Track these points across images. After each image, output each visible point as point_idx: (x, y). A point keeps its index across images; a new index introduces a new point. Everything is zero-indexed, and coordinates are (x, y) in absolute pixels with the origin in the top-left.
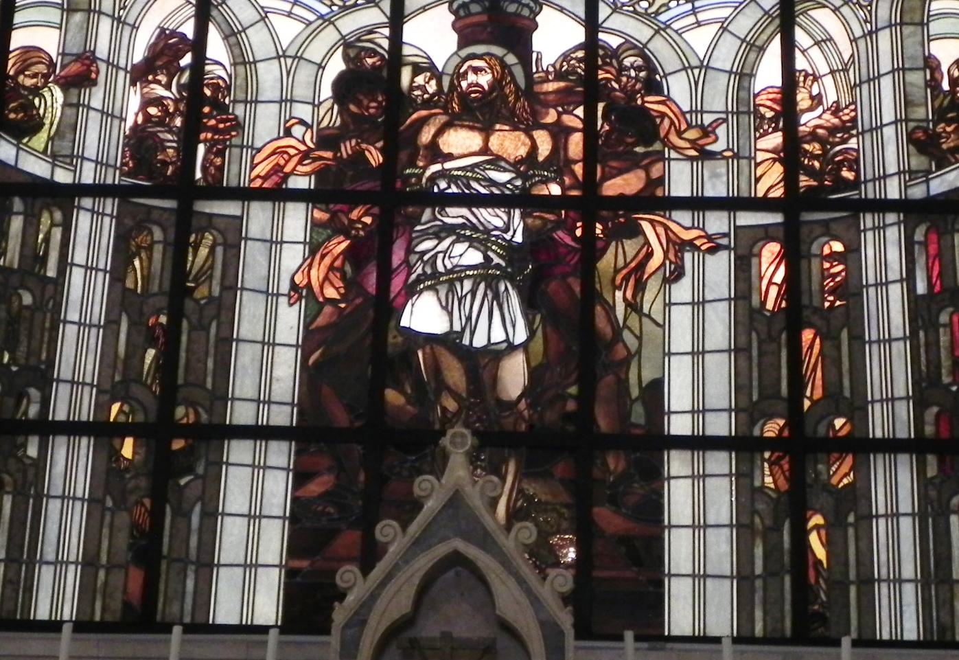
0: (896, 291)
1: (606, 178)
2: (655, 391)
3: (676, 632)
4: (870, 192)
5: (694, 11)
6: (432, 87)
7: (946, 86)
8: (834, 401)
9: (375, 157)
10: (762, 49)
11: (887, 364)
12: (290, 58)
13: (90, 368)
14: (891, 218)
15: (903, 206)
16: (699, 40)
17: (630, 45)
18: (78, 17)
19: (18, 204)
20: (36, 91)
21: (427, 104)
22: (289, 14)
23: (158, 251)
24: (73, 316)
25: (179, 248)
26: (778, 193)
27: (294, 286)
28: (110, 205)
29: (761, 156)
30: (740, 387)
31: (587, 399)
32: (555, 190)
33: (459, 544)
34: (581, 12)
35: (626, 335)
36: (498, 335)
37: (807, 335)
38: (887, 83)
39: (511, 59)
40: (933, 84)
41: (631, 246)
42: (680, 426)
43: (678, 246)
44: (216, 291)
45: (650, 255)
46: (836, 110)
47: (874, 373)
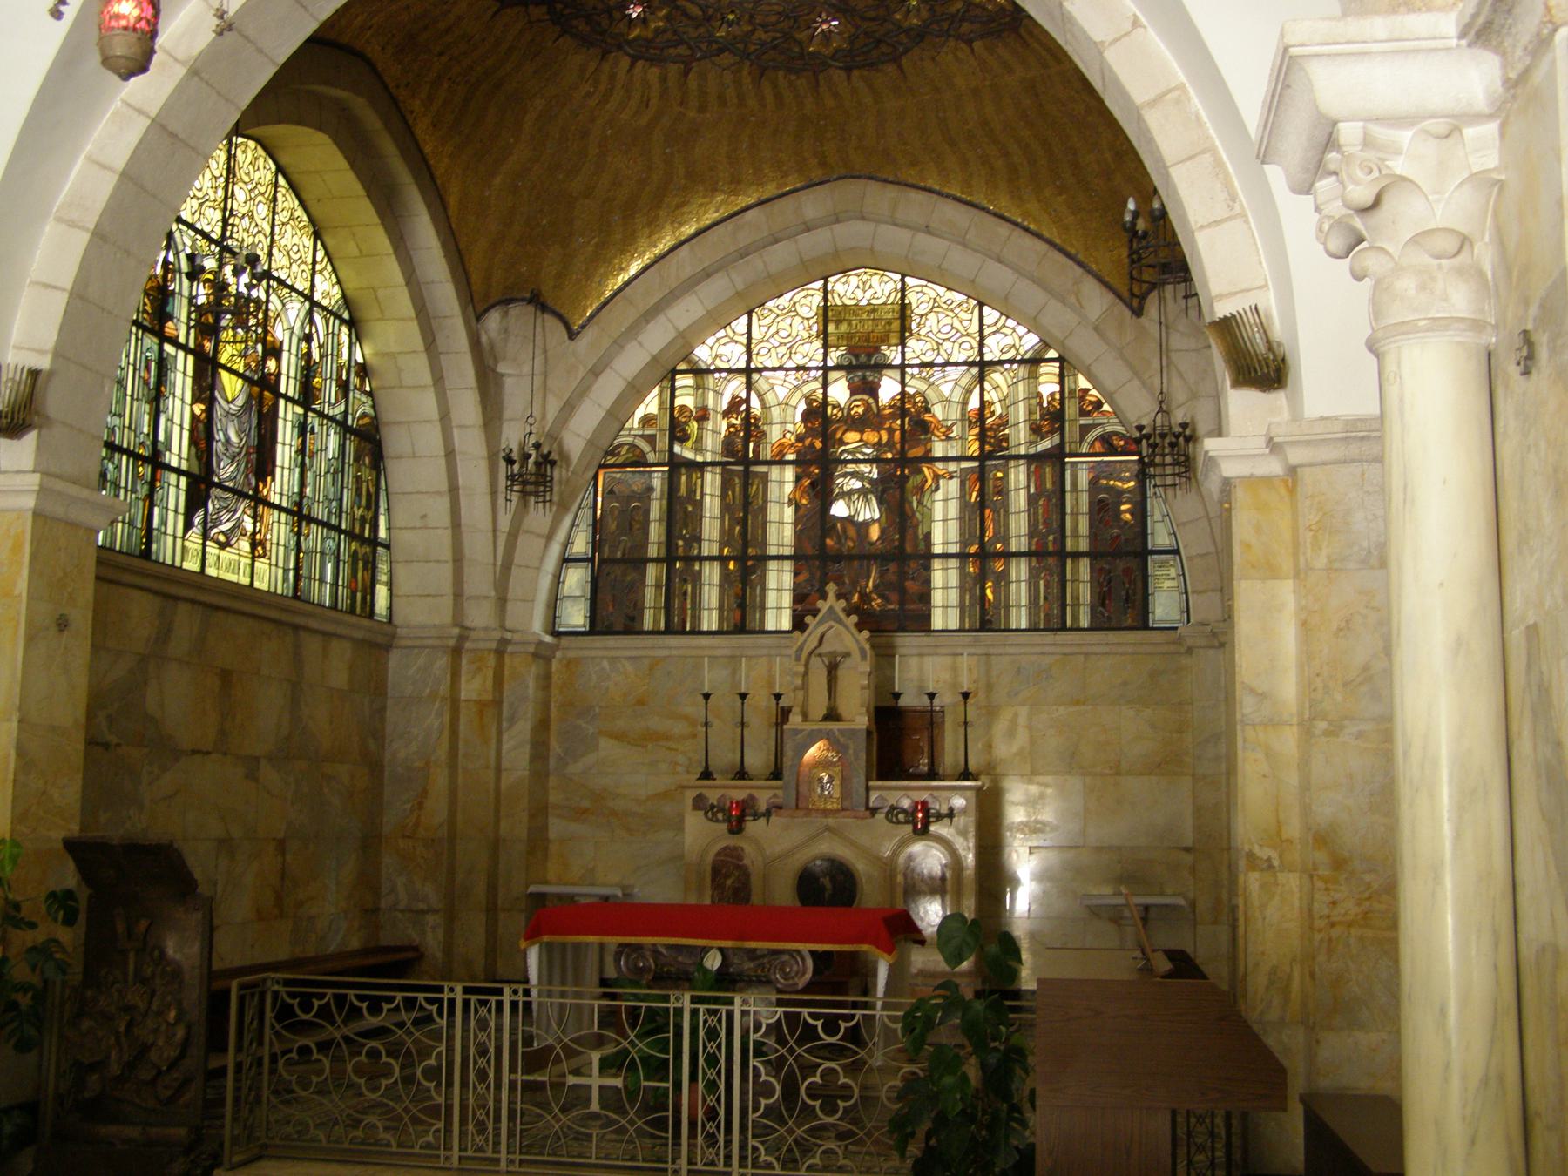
0: (1022, 492)
1: (910, 449)
2: (928, 536)
4: (1013, 452)
6: (840, 414)
7: (1045, 405)
8: (997, 537)
9: (818, 445)
10: (971, 392)
11: (1018, 522)
13: (715, 535)
14: (1021, 462)
15: (1027, 457)
16: (946, 389)
17: (918, 393)
19: (683, 470)
20: (686, 423)
21: (839, 421)
23: (737, 489)
25: (746, 486)
26: (976, 454)
27: (790, 500)
28: (718, 470)
31: (902, 540)
32: (889, 456)
33: (832, 623)
34: (899, 378)
35: (918, 515)
36: (868, 516)
37: (987, 511)
38: (1021, 404)
39: (871, 401)
40: (1040, 404)
41: (919, 478)
42: (937, 550)
43: (937, 477)
44: (760, 502)
46: (1000, 417)
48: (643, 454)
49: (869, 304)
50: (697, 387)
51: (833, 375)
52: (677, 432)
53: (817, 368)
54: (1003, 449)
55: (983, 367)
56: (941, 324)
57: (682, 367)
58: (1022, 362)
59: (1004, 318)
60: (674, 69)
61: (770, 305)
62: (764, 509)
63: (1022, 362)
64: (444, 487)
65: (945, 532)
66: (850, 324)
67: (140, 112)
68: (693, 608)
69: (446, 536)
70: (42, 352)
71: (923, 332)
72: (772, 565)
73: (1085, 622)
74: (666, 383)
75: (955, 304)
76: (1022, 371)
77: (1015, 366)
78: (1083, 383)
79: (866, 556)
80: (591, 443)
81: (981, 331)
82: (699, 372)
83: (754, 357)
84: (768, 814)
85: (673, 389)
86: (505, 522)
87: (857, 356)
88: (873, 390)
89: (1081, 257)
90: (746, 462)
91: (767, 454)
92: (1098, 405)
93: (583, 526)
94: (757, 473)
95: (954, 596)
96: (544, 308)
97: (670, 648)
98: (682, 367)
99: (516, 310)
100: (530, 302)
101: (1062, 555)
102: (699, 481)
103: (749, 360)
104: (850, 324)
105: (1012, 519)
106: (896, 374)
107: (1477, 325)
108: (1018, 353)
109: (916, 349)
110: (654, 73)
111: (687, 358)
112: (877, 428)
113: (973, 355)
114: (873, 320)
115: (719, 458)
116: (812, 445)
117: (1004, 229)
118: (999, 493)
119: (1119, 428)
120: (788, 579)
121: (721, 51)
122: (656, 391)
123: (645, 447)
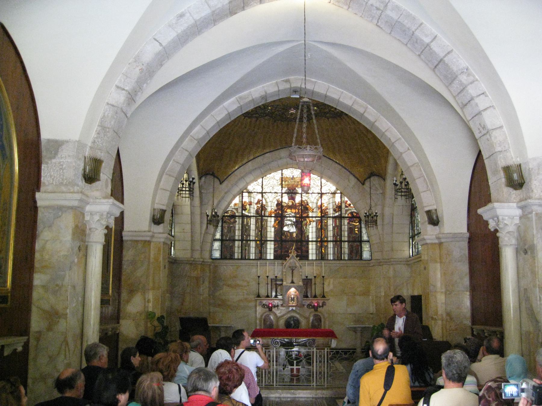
0: (331, 226)
4: (329, 216)
9: (280, 212)
21: (285, 206)
25: (262, 222)
28: (254, 218)
30: (316, 236)
32: (298, 216)
36: (293, 231)
38: (331, 204)
40: (336, 204)
41: (306, 221)
43: (310, 221)
47: (329, 234)
48: (235, 213)
50: (249, 197)
51: (284, 195)
52: (244, 208)
54: (327, 215)
55: (322, 194)
57: (245, 191)
58: (332, 193)
60: (254, 119)
62: (266, 229)
63: (332, 193)
64: (190, 222)
65: (312, 235)
67: (186, 150)
68: (248, 253)
69: (189, 235)
70: (163, 205)
72: (269, 242)
73: (346, 258)
74: (240, 195)
76: (331, 196)
77: (330, 194)
78: (346, 199)
79: (292, 241)
80: (223, 211)
81: (321, 185)
82: (249, 193)
85: (242, 197)
86: (203, 232)
87: (290, 190)
89: (349, 170)
90: (262, 216)
91: (267, 214)
92: (350, 205)
93: (219, 231)
95: (314, 251)
99: (208, 177)
100: (212, 175)
101: (341, 241)
106: (300, 195)
107: (515, 245)
110: (249, 120)
111: (246, 189)
112: (295, 208)
115: (255, 215)
116: (279, 212)
117: (331, 162)
118: (326, 226)
119: (355, 211)
120: (273, 246)
121: (266, 116)
123: (235, 211)
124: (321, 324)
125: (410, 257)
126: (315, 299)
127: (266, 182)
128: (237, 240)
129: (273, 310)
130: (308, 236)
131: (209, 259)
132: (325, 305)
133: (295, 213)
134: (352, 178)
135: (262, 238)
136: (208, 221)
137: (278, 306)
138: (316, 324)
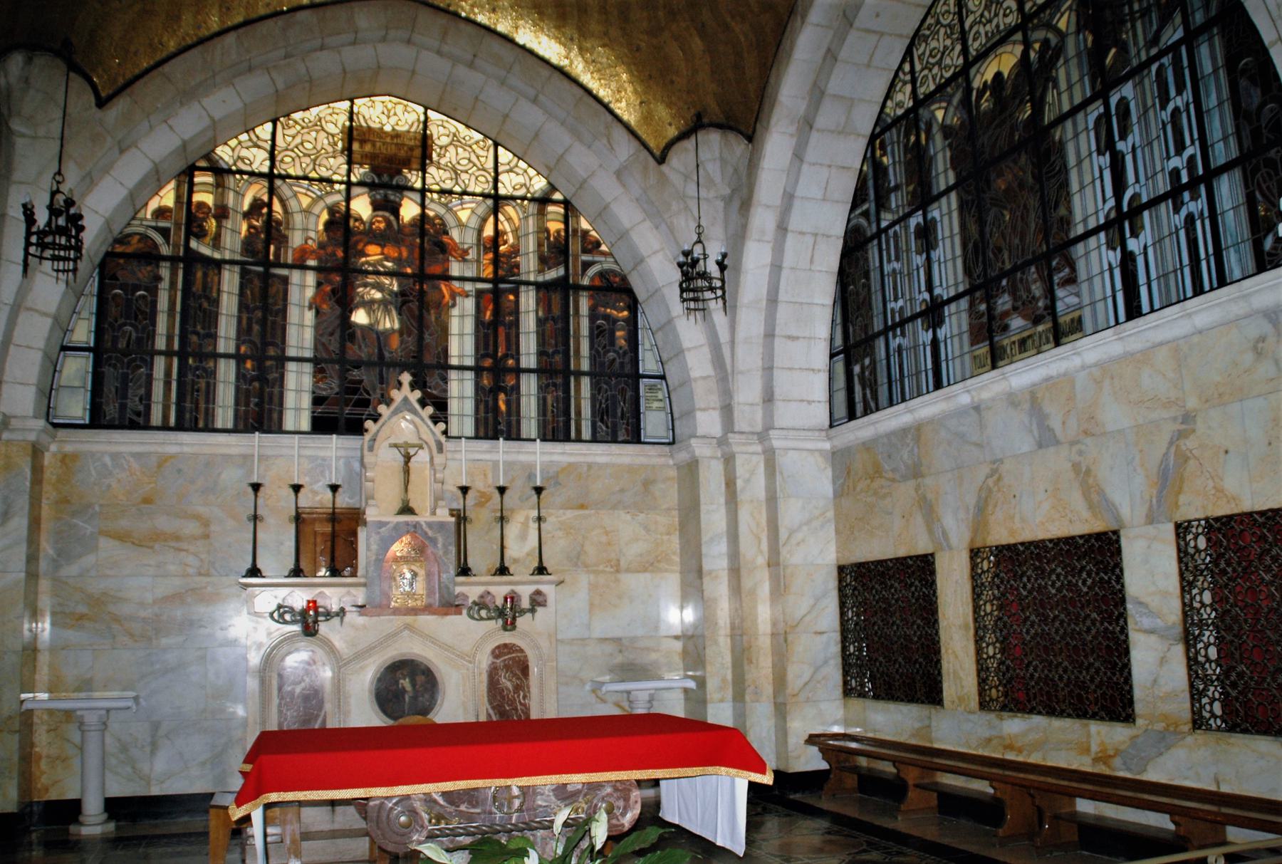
1: (429, 265)
3: (453, 435)
4: (524, 278)
5: (462, 204)
9: (340, 254)
12: (307, 212)
13: (233, 333)
14: (531, 287)
16: (464, 215)
17: (437, 216)
18: (220, 190)
20: (204, 220)
21: (361, 233)
22: (306, 195)
23: (257, 290)
24: (224, 312)
26: (491, 276)
28: (237, 268)
29: (485, 262)
32: (409, 271)
36: (388, 325)
37: (502, 331)
38: (531, 237)
39: (392, 218)
40: (548, 238)
45: (444, 297)
46: (512, 246)
48: (156, 246)
49: (394, 129)
51: (355, 190)
53: (341, 183)
55: (497, 201)
56: (459, 158)
58: (533, 200)
59: (516, 159)
61: (297, 116)
62: (284, 312)
63: (533, 200)
65: (461, 345)
66: (374, 145)
71: (443, 161)
72: (291, 366)
73: (586, 433)
75: (472, 141)
76: (533, 208)
77: (526, 202)
80: (108, 224)
82: (220, 172)
83: (277, 164)
84: (342, 613)
85: (191, 185)
87: (379, 176)
88: (395, 210)
89: (612, 106)
90: (267, 264)
93: (85, 314)
94: (275, 275)
95: (469, 406)
96: (73, 67)
97: (181, 444)
98: (203, 164)
101: (566, 373)
102: (216, 279)
103: (272, 166)
104: (374, 145)
105: (522, 339)
106: (417, 197)
108: (528, 191)
109: (437, 177)
113: (488, 188)
114: (397, 144)
115: (238, 257)
116: (334, 254)
118: (510, 314)
119: (614, 267)
120: (307, 381)
122: (172, 185)
123: (159, 239)
124: (528, 688)
125: (831, 426)
126: (505, 578)
127: (289, 139)
128: (160, 353)
129: (323, 628)
130: (445, 352)
131: (35, 417)
132: (543, 604)
133: (398, 261)
134: (620, 134)
135: (264, 351)
136: (29, 234)
137: (342, 613)
138: (509, 685)
